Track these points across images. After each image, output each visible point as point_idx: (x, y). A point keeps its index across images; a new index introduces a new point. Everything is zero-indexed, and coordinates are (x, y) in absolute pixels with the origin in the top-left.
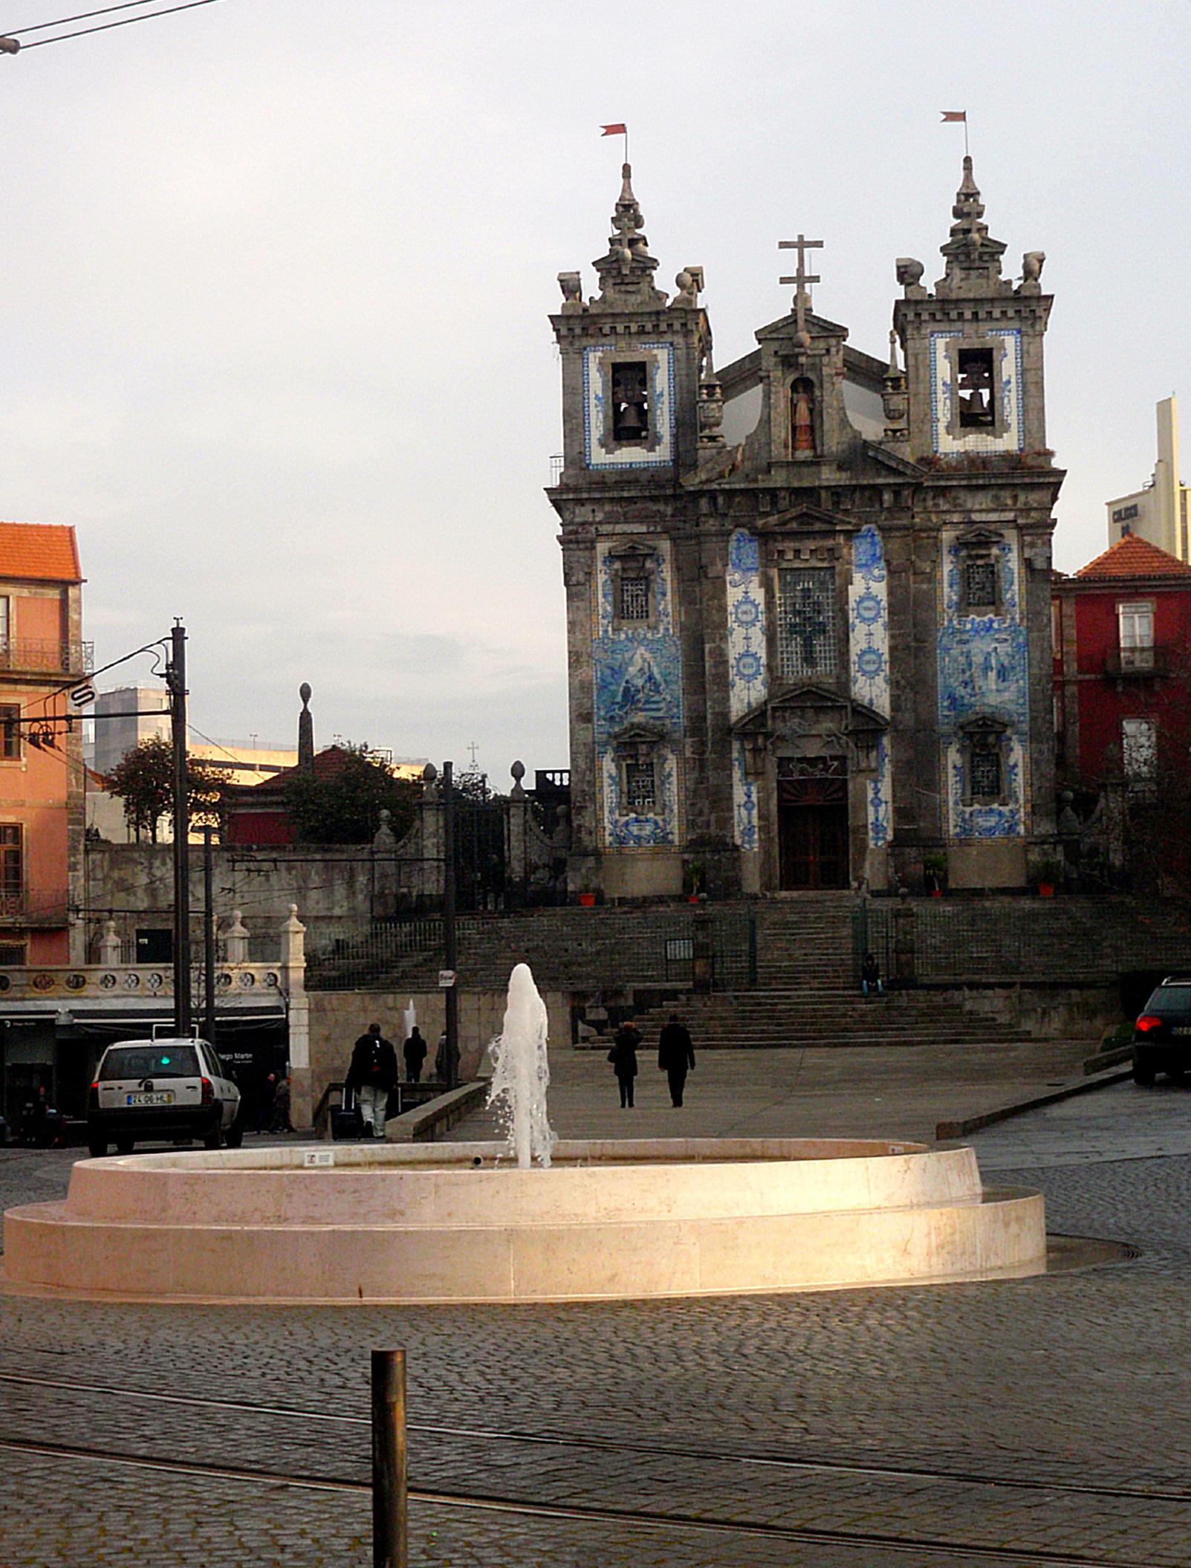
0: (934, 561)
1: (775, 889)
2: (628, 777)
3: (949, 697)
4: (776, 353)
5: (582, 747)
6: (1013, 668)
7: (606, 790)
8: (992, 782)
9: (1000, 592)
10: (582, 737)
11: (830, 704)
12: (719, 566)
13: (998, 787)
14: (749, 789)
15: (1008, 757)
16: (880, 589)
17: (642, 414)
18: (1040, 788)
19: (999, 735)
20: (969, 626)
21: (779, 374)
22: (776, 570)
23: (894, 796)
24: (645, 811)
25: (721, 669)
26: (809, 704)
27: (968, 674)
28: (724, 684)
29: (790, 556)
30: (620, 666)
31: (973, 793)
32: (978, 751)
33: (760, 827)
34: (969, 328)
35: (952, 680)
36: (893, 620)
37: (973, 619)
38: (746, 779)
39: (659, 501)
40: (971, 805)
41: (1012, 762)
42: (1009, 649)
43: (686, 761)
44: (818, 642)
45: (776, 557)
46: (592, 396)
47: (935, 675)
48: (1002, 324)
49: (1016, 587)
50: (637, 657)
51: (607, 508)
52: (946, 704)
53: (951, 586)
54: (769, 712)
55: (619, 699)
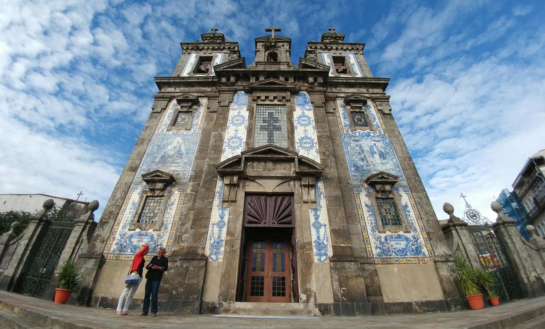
0: (335, 109)
1: (230, 299)
2: (144, 204)
3: (354, 166)
4: (262, 46)
5: (124, 185)
6: (387, 153)
7: (127, 211)
8: (394, 216)
9: (370, 121)
10: (126, 179)
11: (283, 156)
12: (228, 103)
13: (399, 220)
14: (223, 213)
15: (400, 200)
16: (311, 114)
17: (208, 70)
18: (428, 221)
19: (392, 184)
20: (357, 134)
21: (264, 50)
22: (256, 104)
23: (330, 221)
24: (147, 228)
25: (219, 143)
26: (269, 156)
27: (363, 155)
28: (218, 150)
29: (263, 98)
30: (164, 146)
31: (383, 224)
32: (380, 196)
33: (226, 241)
34: (335, 51)
35: (354, 157)
36: (318, 125)
37: (359, 132)
38: (222, 204)
39: (205, 86)
40: (385, 232)
41: (404, 204)
42: (383, 145)
43: (186, 195)
44: (276, 133)
45: (256, 99)
46: (190, 63)
47: (344, 155)
48: (348, 52)
49: (377, 120)
50: (176, 141)
51: (182, 88)
52: (353, 169)
53: (345, 118)
54: (243, 160)
55: (157, 160)
